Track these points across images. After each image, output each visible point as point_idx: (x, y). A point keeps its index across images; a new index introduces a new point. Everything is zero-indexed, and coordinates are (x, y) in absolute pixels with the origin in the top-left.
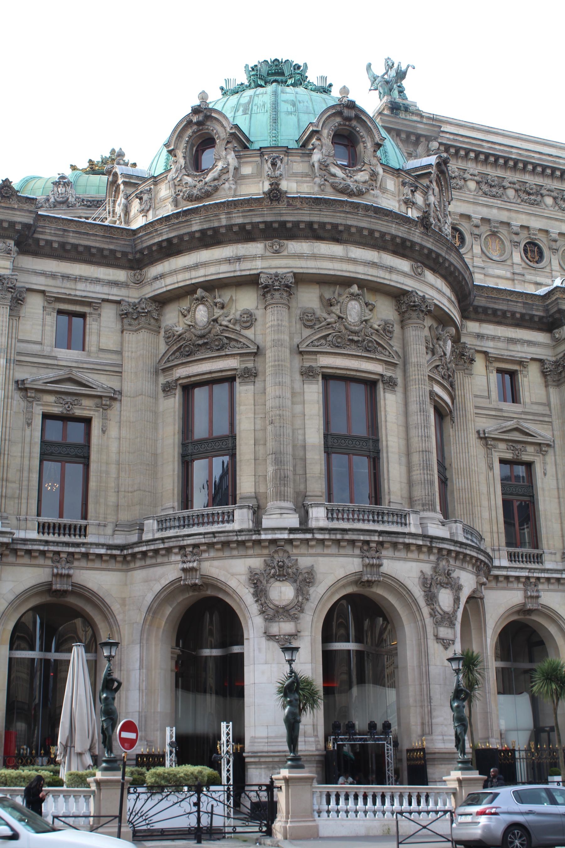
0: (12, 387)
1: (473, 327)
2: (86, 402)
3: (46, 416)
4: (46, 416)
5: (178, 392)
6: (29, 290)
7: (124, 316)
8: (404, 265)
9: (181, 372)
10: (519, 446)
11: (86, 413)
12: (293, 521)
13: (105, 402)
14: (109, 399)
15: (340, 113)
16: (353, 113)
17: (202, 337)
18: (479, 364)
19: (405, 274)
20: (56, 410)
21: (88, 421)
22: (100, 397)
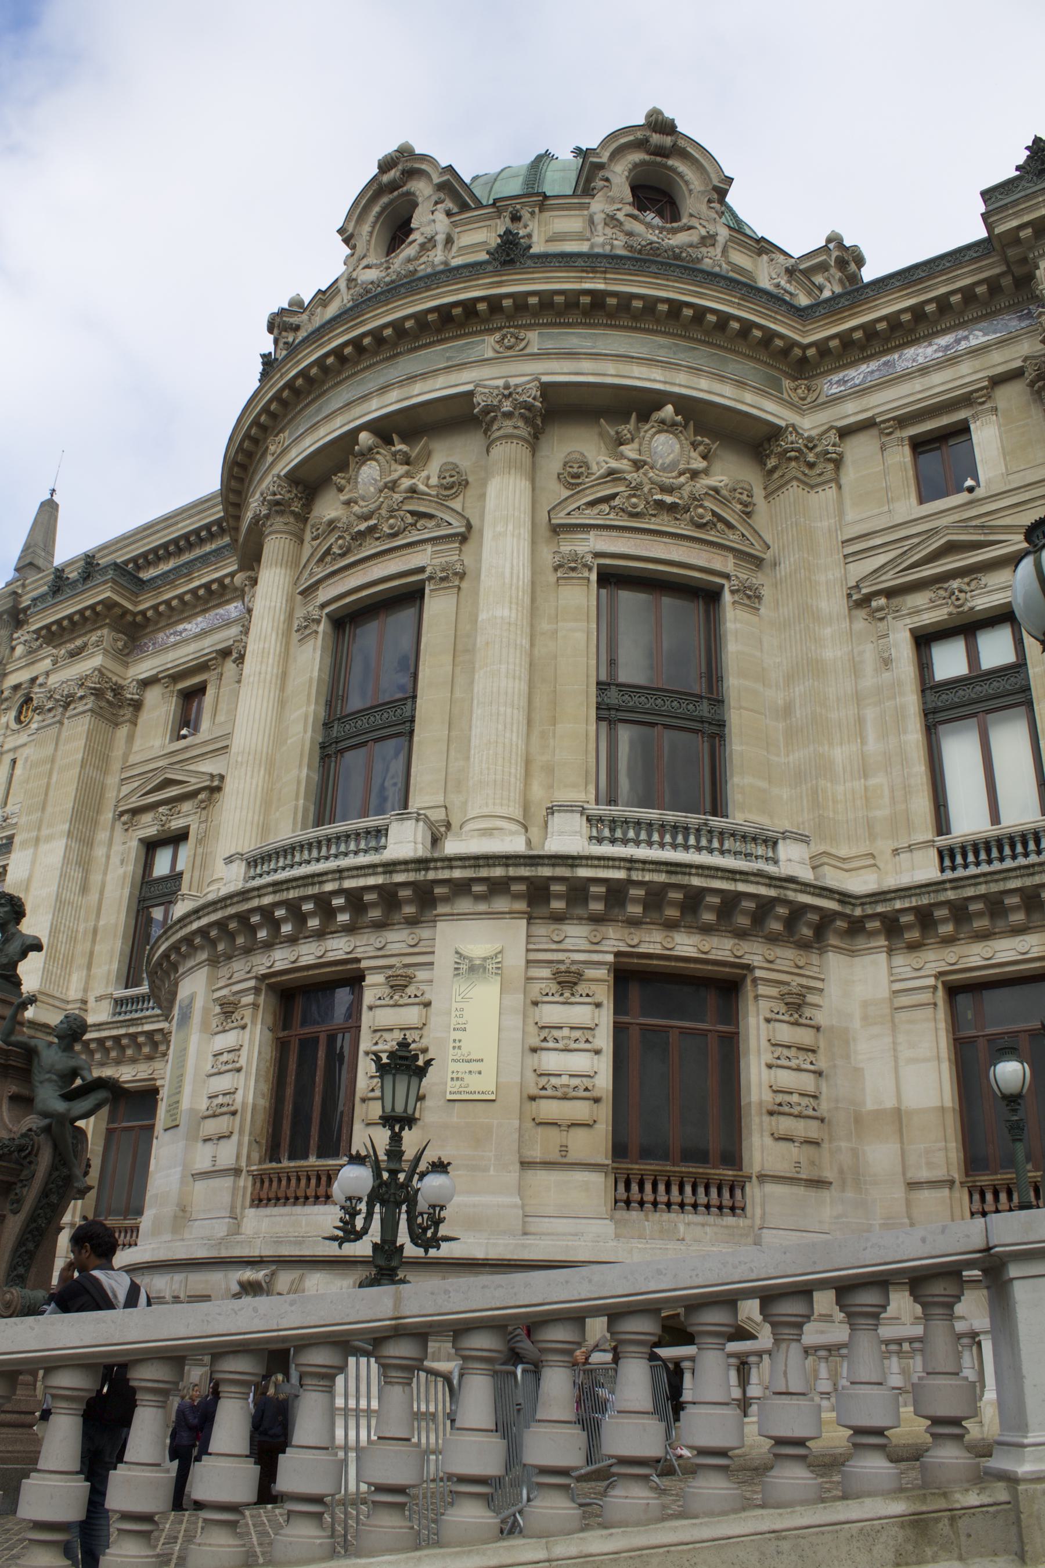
2: (186, 807)
10: (955, 584)
13: (202, 796)
18: (860, 452)
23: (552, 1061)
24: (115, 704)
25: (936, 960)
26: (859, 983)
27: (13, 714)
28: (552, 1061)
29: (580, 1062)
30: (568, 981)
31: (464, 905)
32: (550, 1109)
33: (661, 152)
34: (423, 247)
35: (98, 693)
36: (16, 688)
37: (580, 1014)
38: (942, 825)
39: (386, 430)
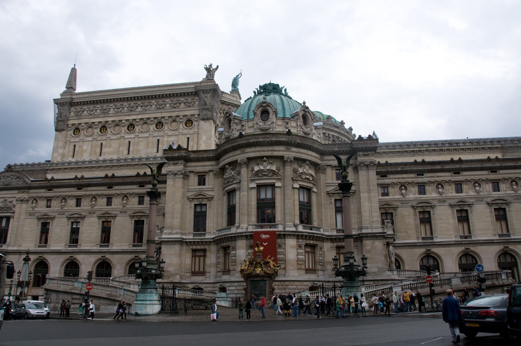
0: (186, 199)
1: (326, 158)
3: (195, 205)
4: (195, 205)
5: (226, 194)
6: (190, 172)
7: (215, 175)
8: (282, 148)
9: (226, 189)
11: (205, 203)
12: (244, 230)
14: (211, 199)
15: (262, 106)
16: (265, 105)
17: (229, 178)
19: (283, 151)
20: (198, 203)
21: (206, 204)
22: (208, 198)
23: (299, 257)
24: (186, 176)
25: (335, 244)
26: (327, 246)
27: (72, 132)
28: (299, 257)
29: (302, 257)
30: (300, 247)
31: (289, 237)
32: (299, 262)
33: (306, 112)
34: (272, 123)
35: (182, 174)
36: (73, 125)
37: (302, 251)
38: (336, 227)
39: (267, 157)
